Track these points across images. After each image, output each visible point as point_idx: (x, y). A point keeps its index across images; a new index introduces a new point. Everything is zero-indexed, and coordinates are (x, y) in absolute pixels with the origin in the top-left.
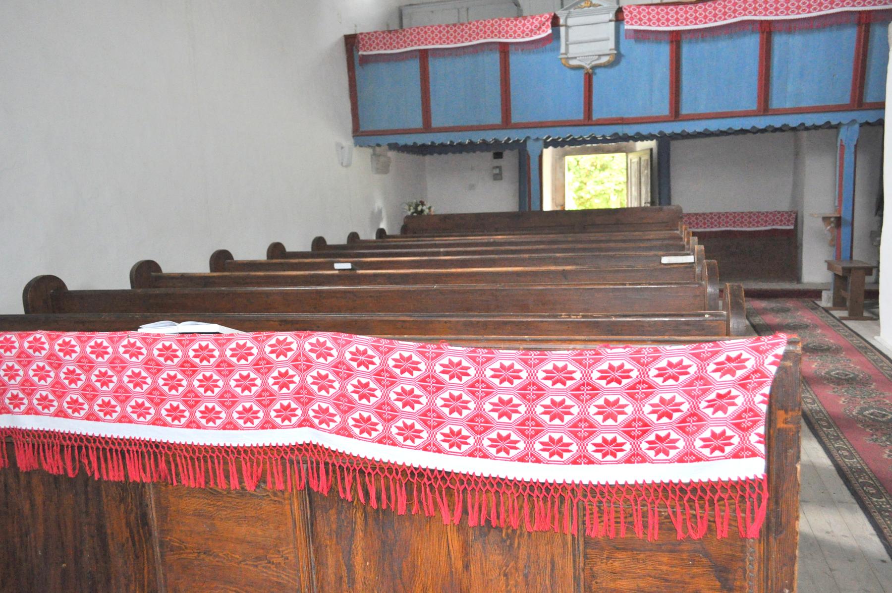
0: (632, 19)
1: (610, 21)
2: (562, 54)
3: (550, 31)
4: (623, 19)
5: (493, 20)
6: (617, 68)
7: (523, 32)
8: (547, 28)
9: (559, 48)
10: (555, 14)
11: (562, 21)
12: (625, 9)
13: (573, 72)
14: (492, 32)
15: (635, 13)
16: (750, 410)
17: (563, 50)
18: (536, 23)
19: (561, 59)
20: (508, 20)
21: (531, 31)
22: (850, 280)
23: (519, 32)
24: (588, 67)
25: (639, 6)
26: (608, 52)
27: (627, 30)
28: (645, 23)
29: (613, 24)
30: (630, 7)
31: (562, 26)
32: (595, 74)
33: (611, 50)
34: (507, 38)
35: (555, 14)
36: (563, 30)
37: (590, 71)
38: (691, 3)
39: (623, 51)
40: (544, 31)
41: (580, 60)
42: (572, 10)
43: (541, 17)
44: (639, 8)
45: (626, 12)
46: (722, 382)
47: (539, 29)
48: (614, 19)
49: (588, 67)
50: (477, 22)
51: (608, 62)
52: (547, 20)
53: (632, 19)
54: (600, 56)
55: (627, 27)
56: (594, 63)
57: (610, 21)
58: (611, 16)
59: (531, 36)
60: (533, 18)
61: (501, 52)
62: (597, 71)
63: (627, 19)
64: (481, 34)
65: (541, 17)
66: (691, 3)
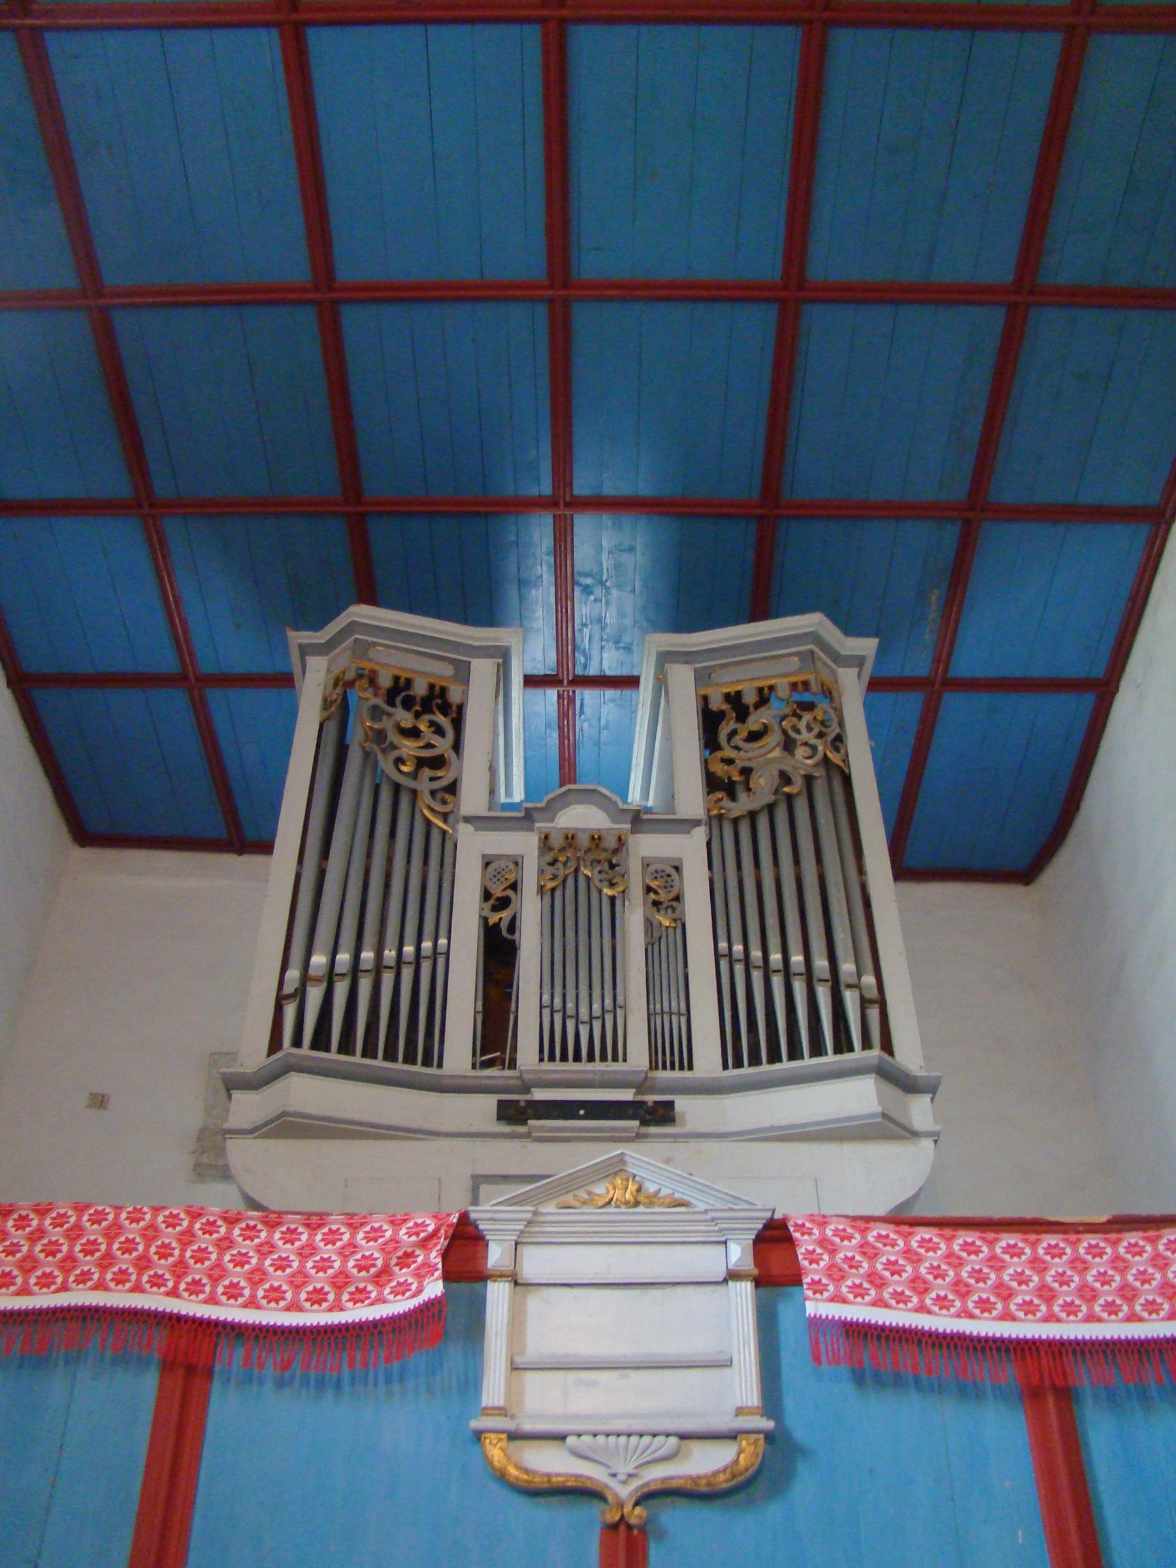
0: (836, 1274)
1: (733, 1276)
2: (487, 1411)
3: (434, 1288)
4: (795, 1279)
5: (156, 1210)
6: (774, 1511)
7: (299, 1280)
8: (420, 1277)
9: (471, 1383)
10: (464, 1217)
11: (496, 1255)
12: (800, 1227)
13: (543, 1513)
14: (143, 1263)
15: (848, 1249)
17: (493, 1391)
18: (370, 1249)
19: (478, 1435)
20: (231, 1221)
21: (341, 1281)
23: (278, 1279)
24: (625, 1492)
25: (867, 1221)
26: (725, 1422)
27: (816, 1323)
28: (900, 1297)
29: (747, 1287)
30: (823, 1222)
31: (499, 1276)
32: (662, 1535)
33: (740, 1411)
34: (212, 1300)
35: (464, 1217)
36: (497, 1294)
37: (636, 1515)
38: (1092, 1228)
39: (799, 1432)
40: (402, 1289)
41: (577, 1454)
42: (549, 1208)
43: (396, 1223)
44: (864, 1231)
45: (805, 1244)
47: (384, 1274)
48: (749, 1265)
49: (625, 1492)
50: (80, 1209)
51: (732, 1469)
52: (425, 1244)
53: (836, 1274)
54: (684, 1437)
55: (818, 1307)
56: (656, 1474)
57: (733, 1276)
58: (739, 1253)
59: (337, 1307)
60: (354, 1227)
61: (167, 1367)
62: (673, 1517)
63: (813, 1272)
64: (87, 1263)
65: (396, 1223)
66: (1092, 1228)
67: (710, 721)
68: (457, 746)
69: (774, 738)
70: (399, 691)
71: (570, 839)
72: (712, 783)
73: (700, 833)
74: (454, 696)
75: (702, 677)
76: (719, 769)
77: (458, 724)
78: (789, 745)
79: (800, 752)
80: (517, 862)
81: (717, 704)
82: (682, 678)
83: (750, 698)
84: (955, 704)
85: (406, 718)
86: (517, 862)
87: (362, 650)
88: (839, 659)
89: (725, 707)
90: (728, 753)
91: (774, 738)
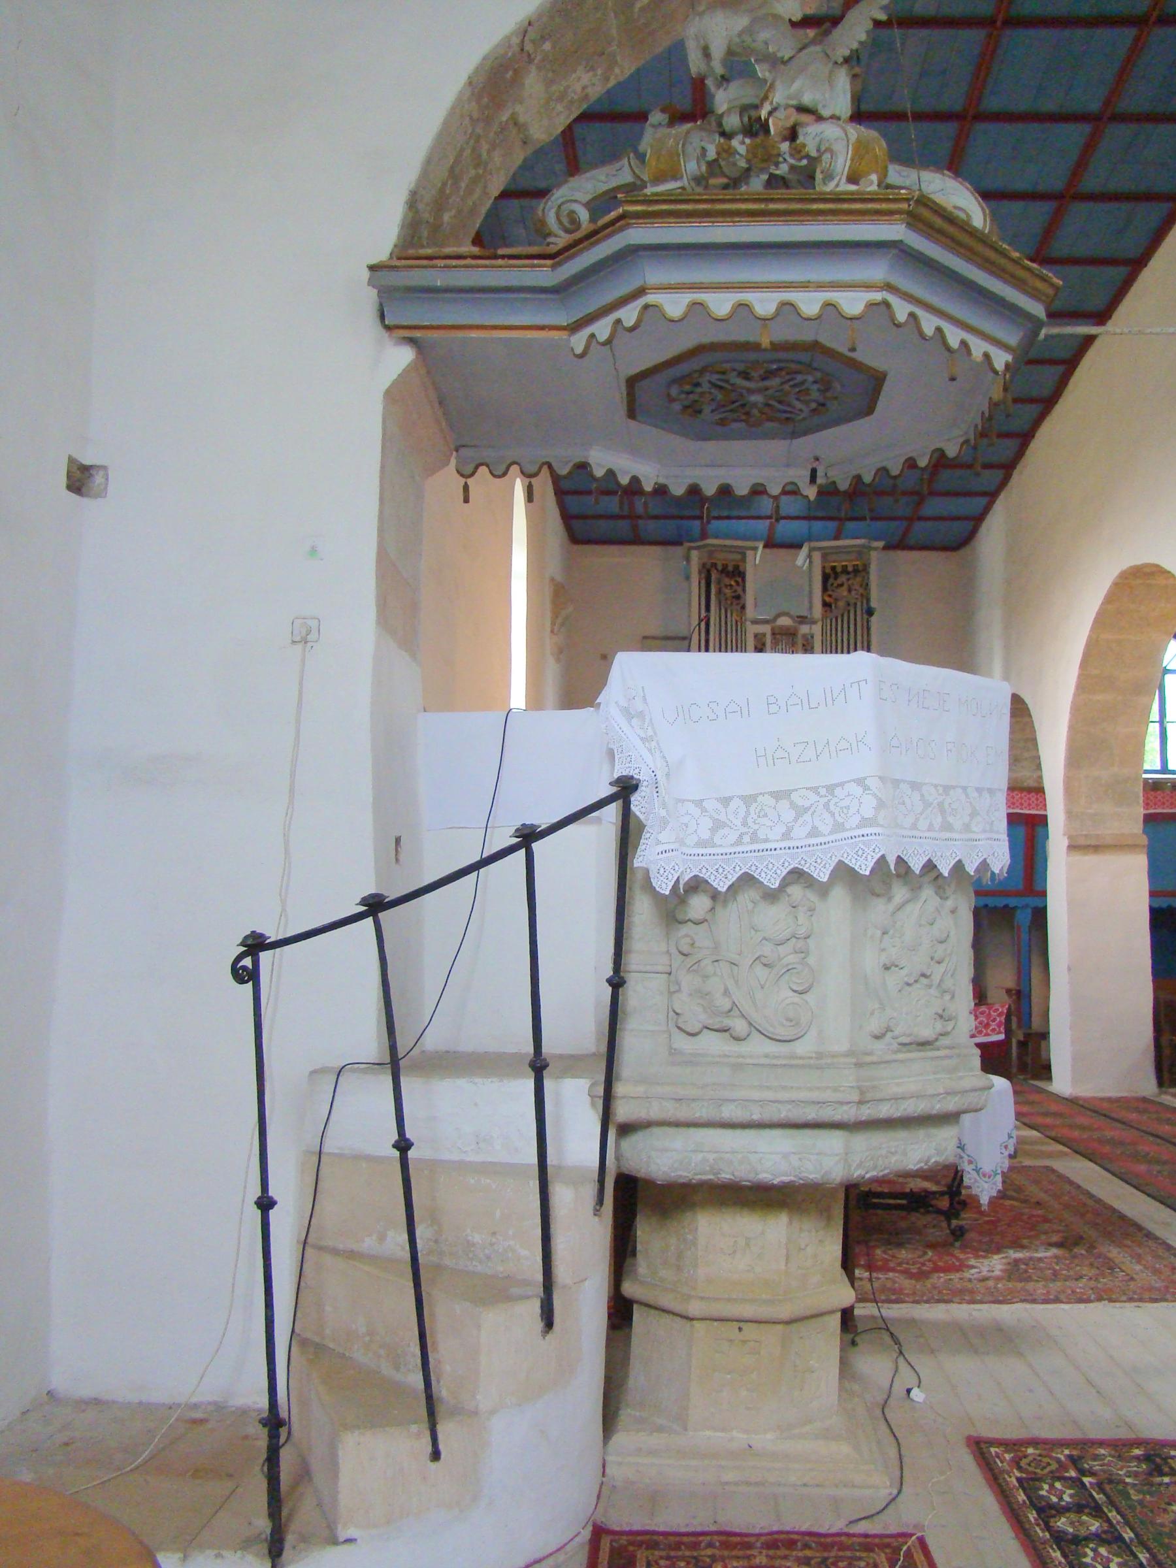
16: (1000, 1021)
22: (1030, 1044)
46: (994, 1014)
67: (825, 578)
68: (744, 590)
69: (845, 586)
70: (724, 571)
71: (781, 627)
72: (825, 605)
73: (820, 624)
74: (741, 569)
75: (824, 557)
76: (827, 599)
77: (744, 580)
78: (850, 591)
79: (853, 593)
80: (764, 635)
81: (828, 571)
82: (817, 556)
83: (839, 570)
84: (918, 526)
85: (727, 581)
86: (764, 635)
87: (711, 553)
88: (870, 548)
89: (831, 572)
90: (830, 593)
91: (845, 586)
